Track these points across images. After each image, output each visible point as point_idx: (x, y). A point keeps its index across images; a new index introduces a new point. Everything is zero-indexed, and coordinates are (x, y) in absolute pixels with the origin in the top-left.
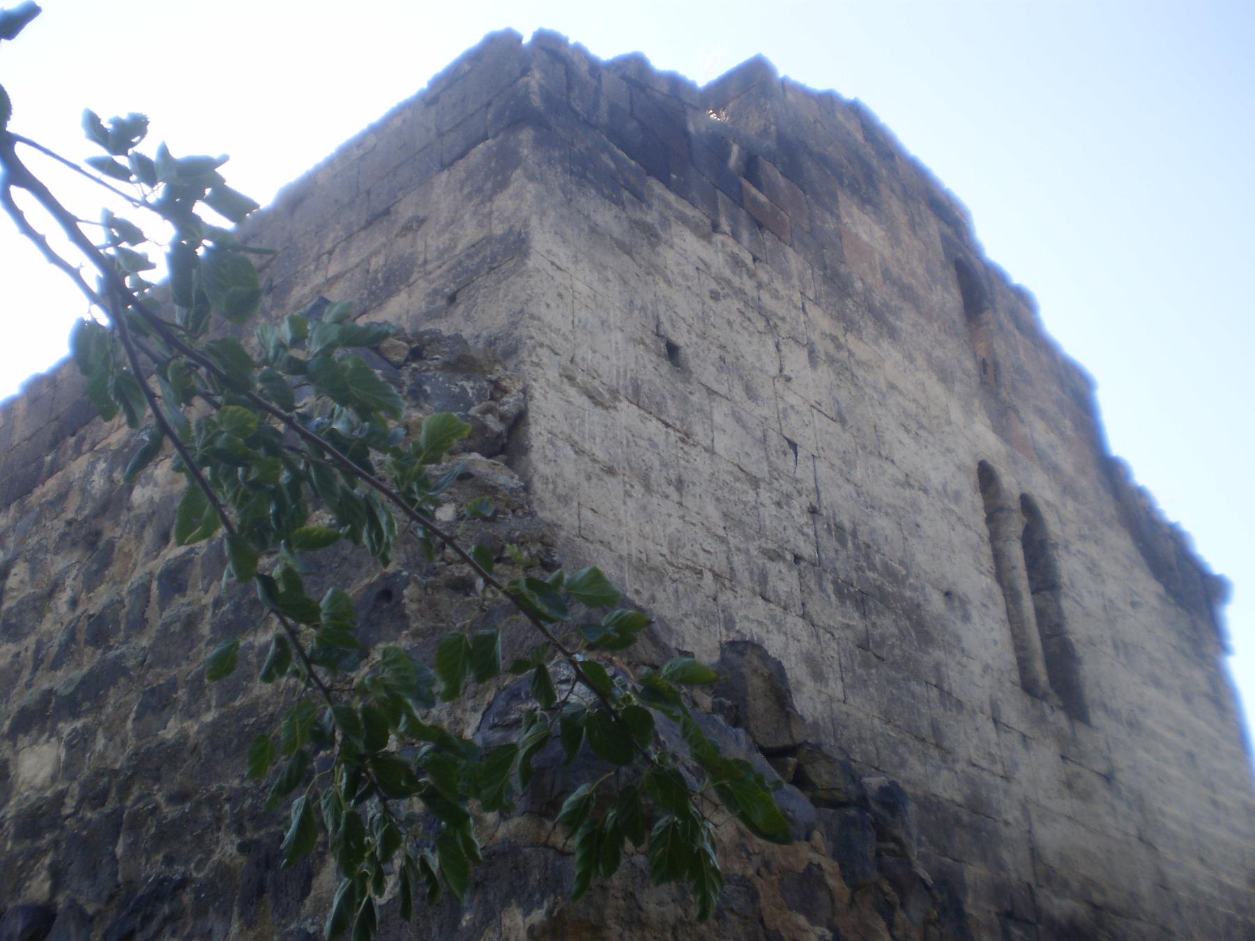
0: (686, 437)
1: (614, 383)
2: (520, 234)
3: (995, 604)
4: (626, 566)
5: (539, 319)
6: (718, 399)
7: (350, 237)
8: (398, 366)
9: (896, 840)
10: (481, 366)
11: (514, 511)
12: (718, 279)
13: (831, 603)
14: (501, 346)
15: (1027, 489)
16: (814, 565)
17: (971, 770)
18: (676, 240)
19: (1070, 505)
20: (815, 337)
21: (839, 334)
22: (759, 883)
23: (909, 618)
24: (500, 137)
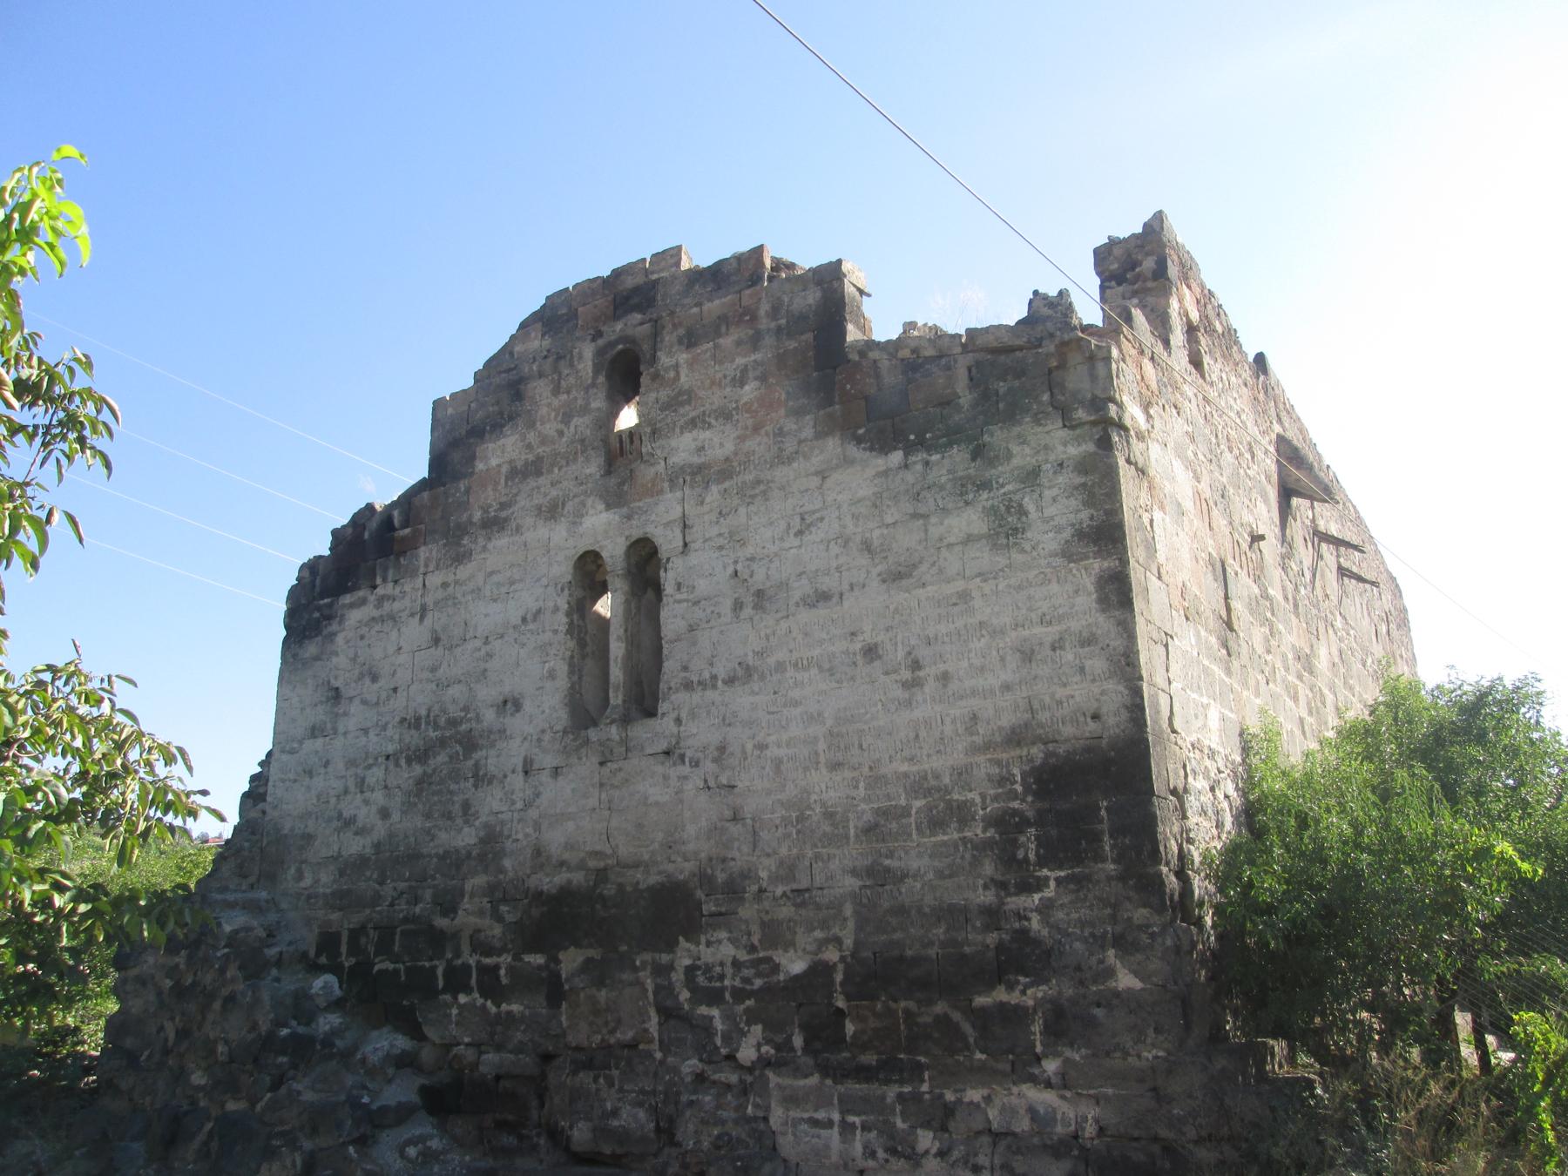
23: (461, 744)
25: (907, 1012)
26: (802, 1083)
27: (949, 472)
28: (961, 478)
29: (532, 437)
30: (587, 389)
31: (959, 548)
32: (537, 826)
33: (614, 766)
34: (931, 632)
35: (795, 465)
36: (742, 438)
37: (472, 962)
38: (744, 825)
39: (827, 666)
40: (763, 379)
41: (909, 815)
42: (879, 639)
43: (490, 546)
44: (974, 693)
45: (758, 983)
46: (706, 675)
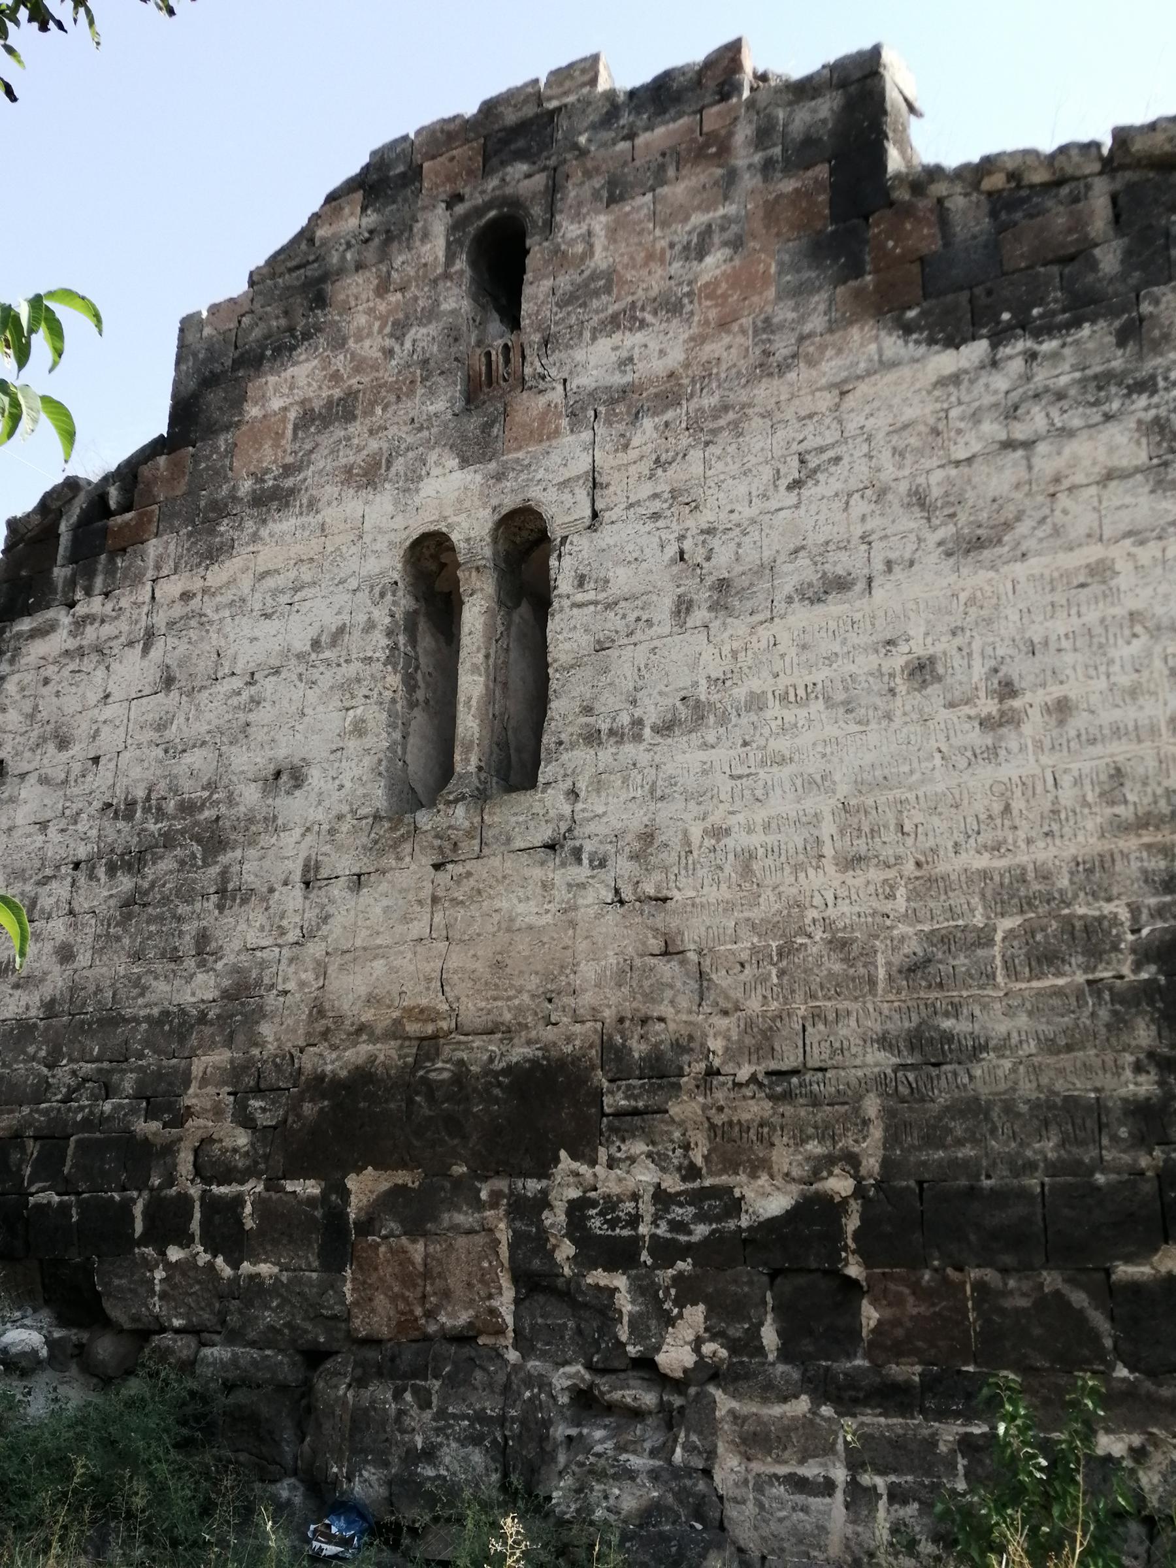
25: (981, 1287)
26: (777, 1410)
27: (1074, 368)
28: (1096, 377)
29: (340, 362)
30: (435, 282)
31: (1093, 490)
32: (322, 970)
33: (458, 869)
34: (1036, 633)
35: (791, 376)
36: (699, 340)
37: (194, 1191)
38: (683, 963)
39: (840, 696)
40: (736, 244)
41: (990, 942)
42: (938, 649)
43: (264, 533)
44: (1117, 732)
45: (701, 1231)
46: (625, 719)
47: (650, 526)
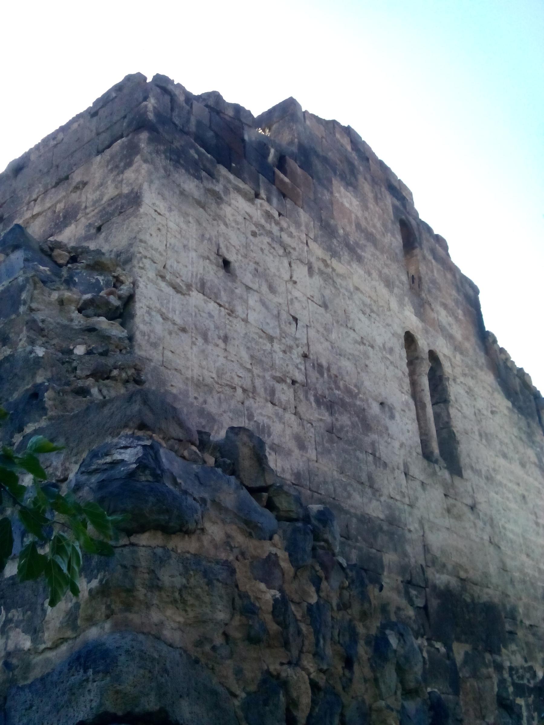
0: (231, 313)
1: (189, 281)
2: (137, 193)
3: (410, 410)
4: (190, 383)
5: (145, 242)
6: (252, 292)
7: (46, 192)
8: (61, 266)
9: (326, 541)
10: (109, 268)
11: (121, 350)
12: (257, 225)
13: (312, 407)
14: (123, 257)
15: (432, 348)
16: (303, 386)
17: (391, 501)
18: (233, 202)
19: (458, 357)
20: (313, 260)
21: (327, 258)
22: (236, 565)
23: (358, 417)
24: (130, 137)
29: (366, 214)
35: (483, 373)
42: (526, 494)
47: (466, 395)
